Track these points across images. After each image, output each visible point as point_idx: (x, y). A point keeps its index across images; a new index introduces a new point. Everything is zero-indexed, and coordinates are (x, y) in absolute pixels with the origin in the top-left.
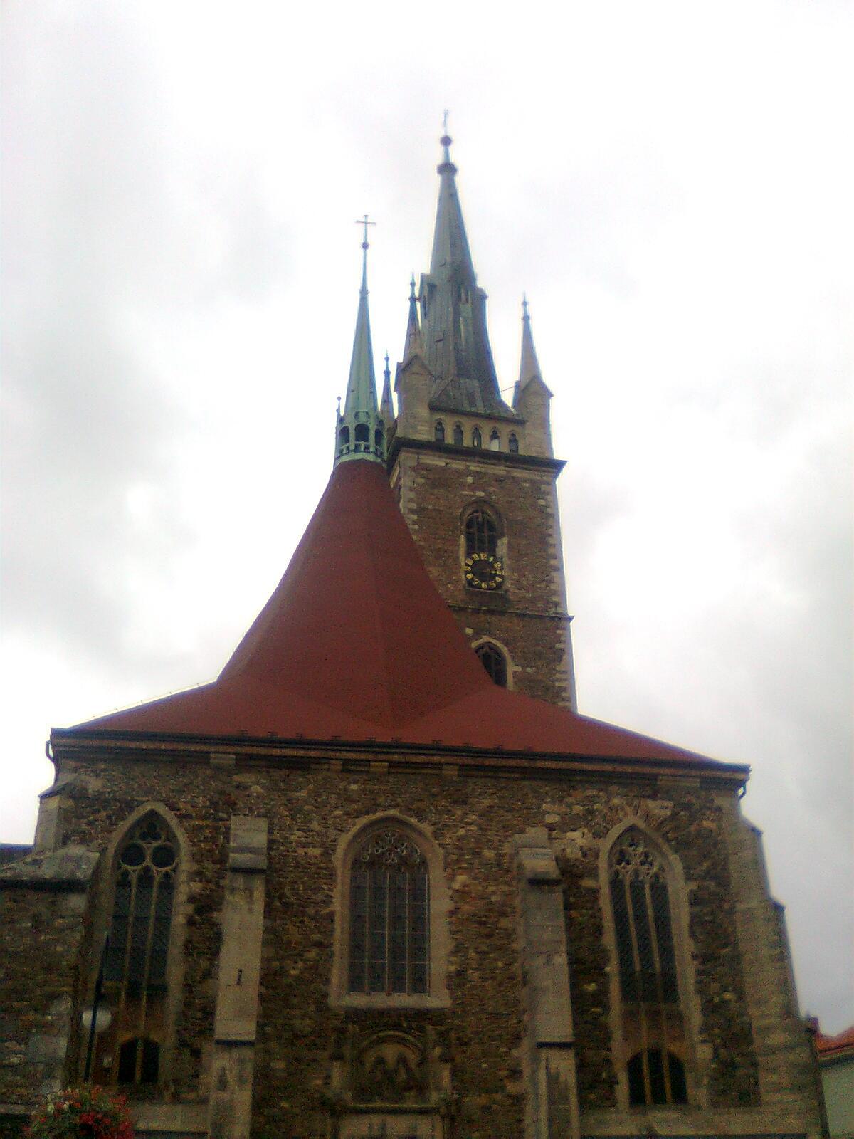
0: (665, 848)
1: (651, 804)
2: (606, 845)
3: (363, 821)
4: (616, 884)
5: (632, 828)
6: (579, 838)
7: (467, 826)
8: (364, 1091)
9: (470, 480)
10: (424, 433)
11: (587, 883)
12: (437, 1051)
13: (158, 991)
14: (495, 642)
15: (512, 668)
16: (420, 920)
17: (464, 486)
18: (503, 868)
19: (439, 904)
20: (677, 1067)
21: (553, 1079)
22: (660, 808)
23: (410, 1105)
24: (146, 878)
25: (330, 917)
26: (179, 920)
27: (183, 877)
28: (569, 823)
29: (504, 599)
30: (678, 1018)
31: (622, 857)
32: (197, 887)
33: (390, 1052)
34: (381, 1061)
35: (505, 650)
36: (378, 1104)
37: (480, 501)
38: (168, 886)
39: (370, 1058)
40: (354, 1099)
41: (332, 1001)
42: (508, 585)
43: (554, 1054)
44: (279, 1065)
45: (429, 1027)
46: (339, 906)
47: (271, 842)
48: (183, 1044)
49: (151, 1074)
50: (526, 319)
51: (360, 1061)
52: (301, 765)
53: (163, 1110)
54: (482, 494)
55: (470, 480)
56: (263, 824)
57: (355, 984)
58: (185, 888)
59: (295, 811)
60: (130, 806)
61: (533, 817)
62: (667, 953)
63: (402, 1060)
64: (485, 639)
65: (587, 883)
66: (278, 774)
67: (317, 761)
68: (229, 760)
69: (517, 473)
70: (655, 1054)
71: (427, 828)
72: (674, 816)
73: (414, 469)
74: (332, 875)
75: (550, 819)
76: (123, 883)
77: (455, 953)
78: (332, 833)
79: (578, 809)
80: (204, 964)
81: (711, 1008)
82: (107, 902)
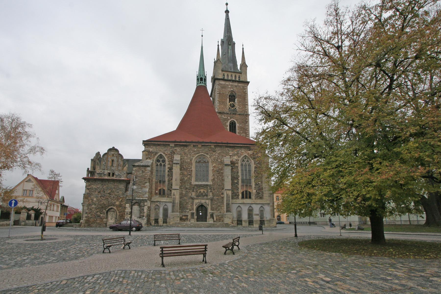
0: (251, 159)
1: (249, 151)
2: (240, 159)
3: (197, 155)
4: (242, 165)
5: (245, 156)
6: (235, 158)
7: (215, 155)
8: (198, 196)
9: (230, 86)
10: (221, 77)
11: (236, 165)
13: (164, 182)
14: (235, 121)
16: (208, 171)
17: (228, 88)
18: (222, 162)
19: (211, 168)
20: (250, 193)
21: (227, 195)
22: (250, 152)
24: (161, 165)
25: (192, 171)
26: (167, 171)
27: (167, 164)
28: (234, 155)
29: (236, 111)
30: (251, 186)
31: (243, 161)
32: (169, 166)
33: (202, 191)
34: (200, 192)
37: (232, 91)
38: (164, 166)
39: (199, 191)
41: (192, 183)
42: (237, 108)
43: (228, 191)
44: (184, 192)
46: (193, 169)
47: (181, 159)
48: (168, 189)
49: (164, 193)
50: (243, 49)
51: (197, 191)
53: (165, 198)
55: (230, 86)
56: (180, 156)
57: (196, 180)
58: (167, 166)
61: (227, 154)
62: (250, 175)
63: (204, 192)
64: (232, 119)
65: (236, 165)
66: (182, 147)
67: (189, 145)
68: (173, 145)
69: (240, 85)
70: (246, 191)
71: (208, 156)
72: (253, 154)
74: (192, 164)
75: (230, 154)
76: (157, 165)
77: (213, 176)
78: (192, 157)
79: (236, 153)
80: (171, 178)
81: (256, 184)
82: (155, 168)
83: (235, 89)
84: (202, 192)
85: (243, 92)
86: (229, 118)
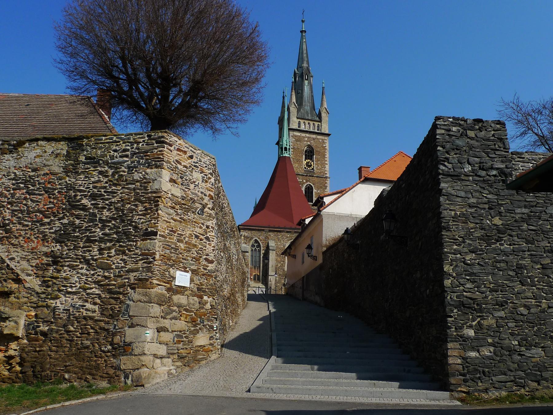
9: (306, 139)
10: (295, 126)
15: (314, 191)
17: (305, 141)
29: (313, 172)
35: (313, 186)
38: (260, 251)
52: (280, 232)
54: (309, 143)
59: (279, 239)
60: (252, 238)
64: (308, 183)
69: (319, 137)
73: (292, 136)
76: (252, 250)
83: (313, 143)
85: (322, 146)
86: (305, 181)
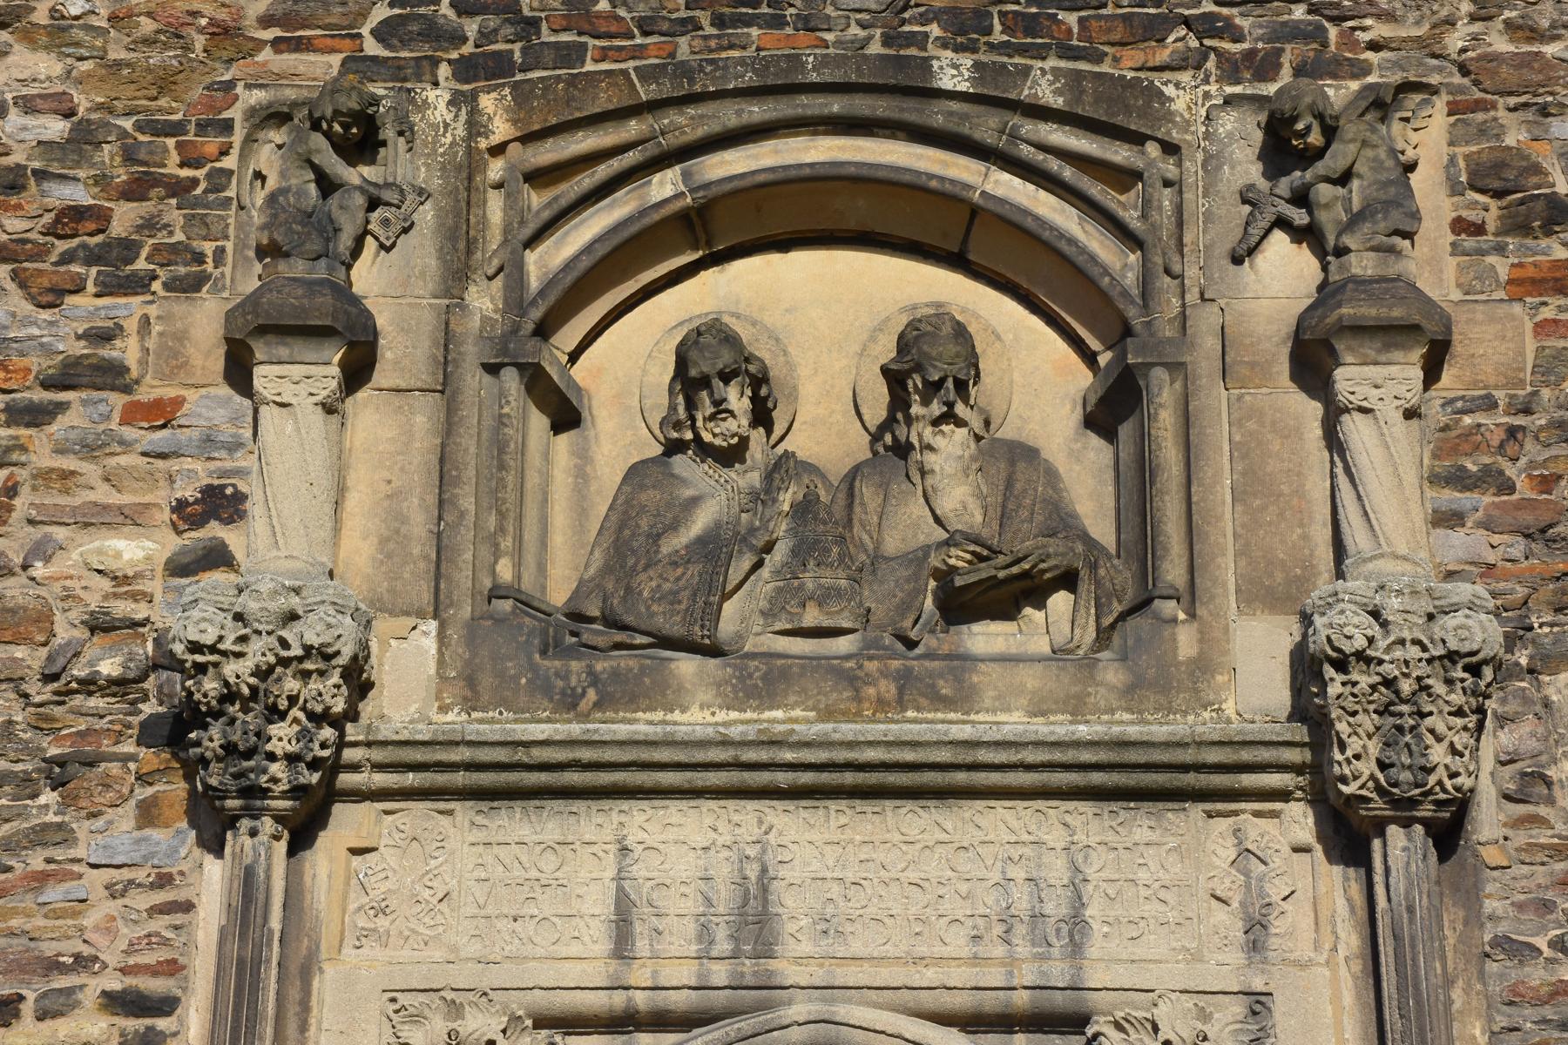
12: (1284, 274)
23: (1005, 718)
36: (698, 709)
39: (626, 363)
40: (467, 683)
45: (1184, 96)
84: (826, 421)
